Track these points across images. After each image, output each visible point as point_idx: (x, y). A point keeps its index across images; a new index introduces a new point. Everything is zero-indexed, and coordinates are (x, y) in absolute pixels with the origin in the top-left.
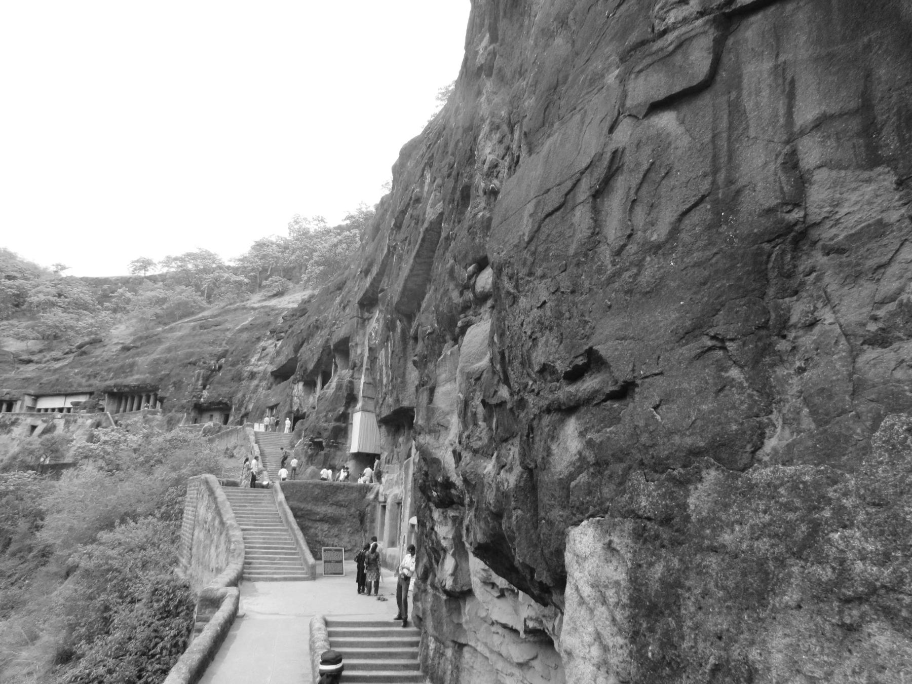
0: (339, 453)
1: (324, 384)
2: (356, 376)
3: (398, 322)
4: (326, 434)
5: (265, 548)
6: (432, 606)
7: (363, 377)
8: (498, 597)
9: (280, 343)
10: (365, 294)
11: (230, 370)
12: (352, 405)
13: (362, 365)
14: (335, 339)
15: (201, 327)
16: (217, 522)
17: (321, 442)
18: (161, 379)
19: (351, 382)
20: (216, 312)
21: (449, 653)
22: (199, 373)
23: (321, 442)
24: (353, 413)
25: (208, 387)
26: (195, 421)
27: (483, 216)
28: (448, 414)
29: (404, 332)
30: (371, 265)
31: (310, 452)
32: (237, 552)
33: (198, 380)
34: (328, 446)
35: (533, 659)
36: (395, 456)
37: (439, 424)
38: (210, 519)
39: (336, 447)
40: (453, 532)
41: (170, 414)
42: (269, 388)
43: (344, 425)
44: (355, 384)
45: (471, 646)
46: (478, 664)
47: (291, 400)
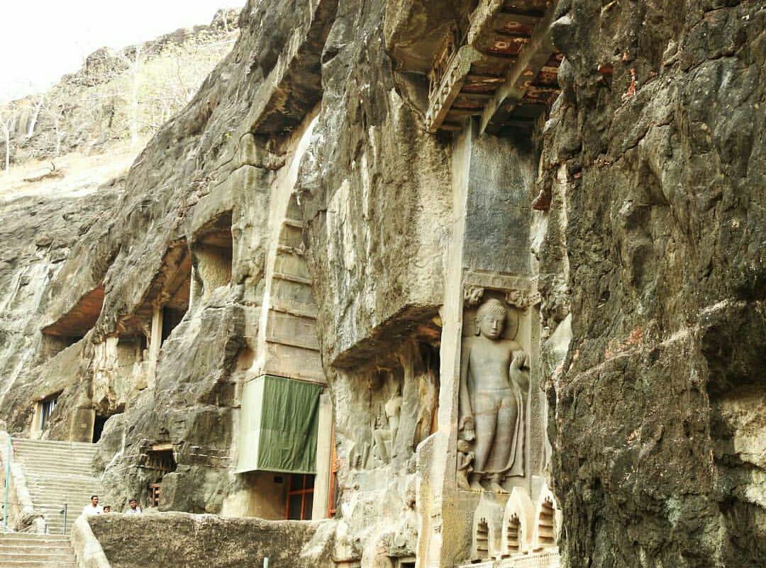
0: (212, 475)
1: (165, 334)
2: (249, 297)
3: (393, 94)
4: (182, 434)
10: (267, 108)
12: (240, 364)
13: (262, 273)
14: (198, 219)
23: (171, 451)
29: (408, 123)
30: (279, 44)
31: (142, 476)
39: (202, 461)
42: (40, 363)
43: (221, 410)
44: (247, 314)
47: (90, 380)
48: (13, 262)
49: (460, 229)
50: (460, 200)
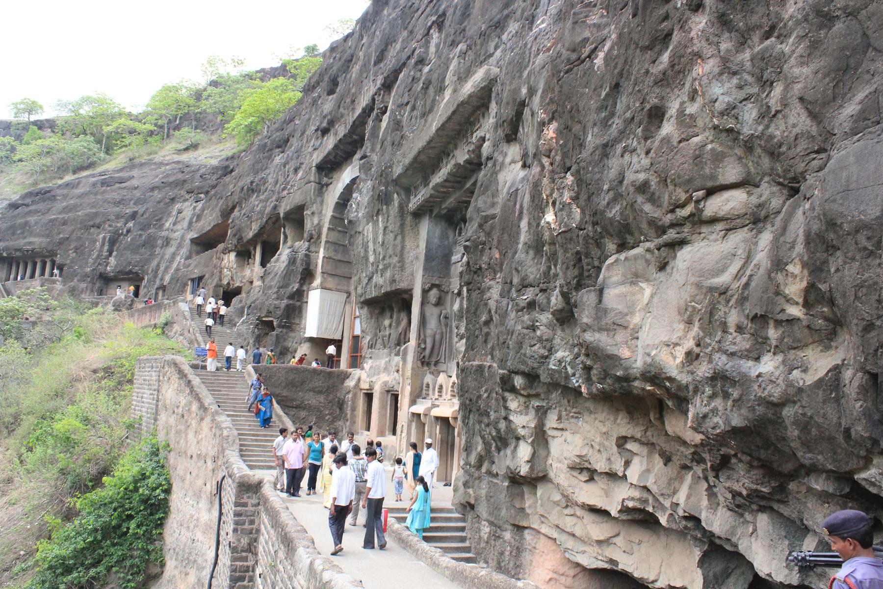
0: (292, 334)
2: (313, 249)
3: (395, 195)
5: (253, 435)
6: (487, 492)
7: (322, 250)
8: (586, 481)
9: (200, 205)
11: (141, 235)
12: (307, 281)
13: (319, 237)
15: (103, 183)
16: (195, 407)
17: (272, 321)
18: (61, 243)
19: (307, 256)
20: (120, 166)
21: (507, 535)
22: (104, 238)
23: (272, 321)
24: (309, 290)
25: (115, 253)
26: (101, 292)
27: (713, 150)
28: (627, 315)
29: (402, 208)
32: (231, 439)
33: (103, 244)
34: (279, 326)
35: (614, 537)
36: (380, 341)
37: (614, 323)
38: (182, 404)
40: (535, 422)
41: (72, 284)
43: (298, 304)
44: (312, 258)
45: (533, 529)
46: (542, 544)
47: (221, 272)
48: (173, 200)
49: (422, 257)
50: (423, 245)
